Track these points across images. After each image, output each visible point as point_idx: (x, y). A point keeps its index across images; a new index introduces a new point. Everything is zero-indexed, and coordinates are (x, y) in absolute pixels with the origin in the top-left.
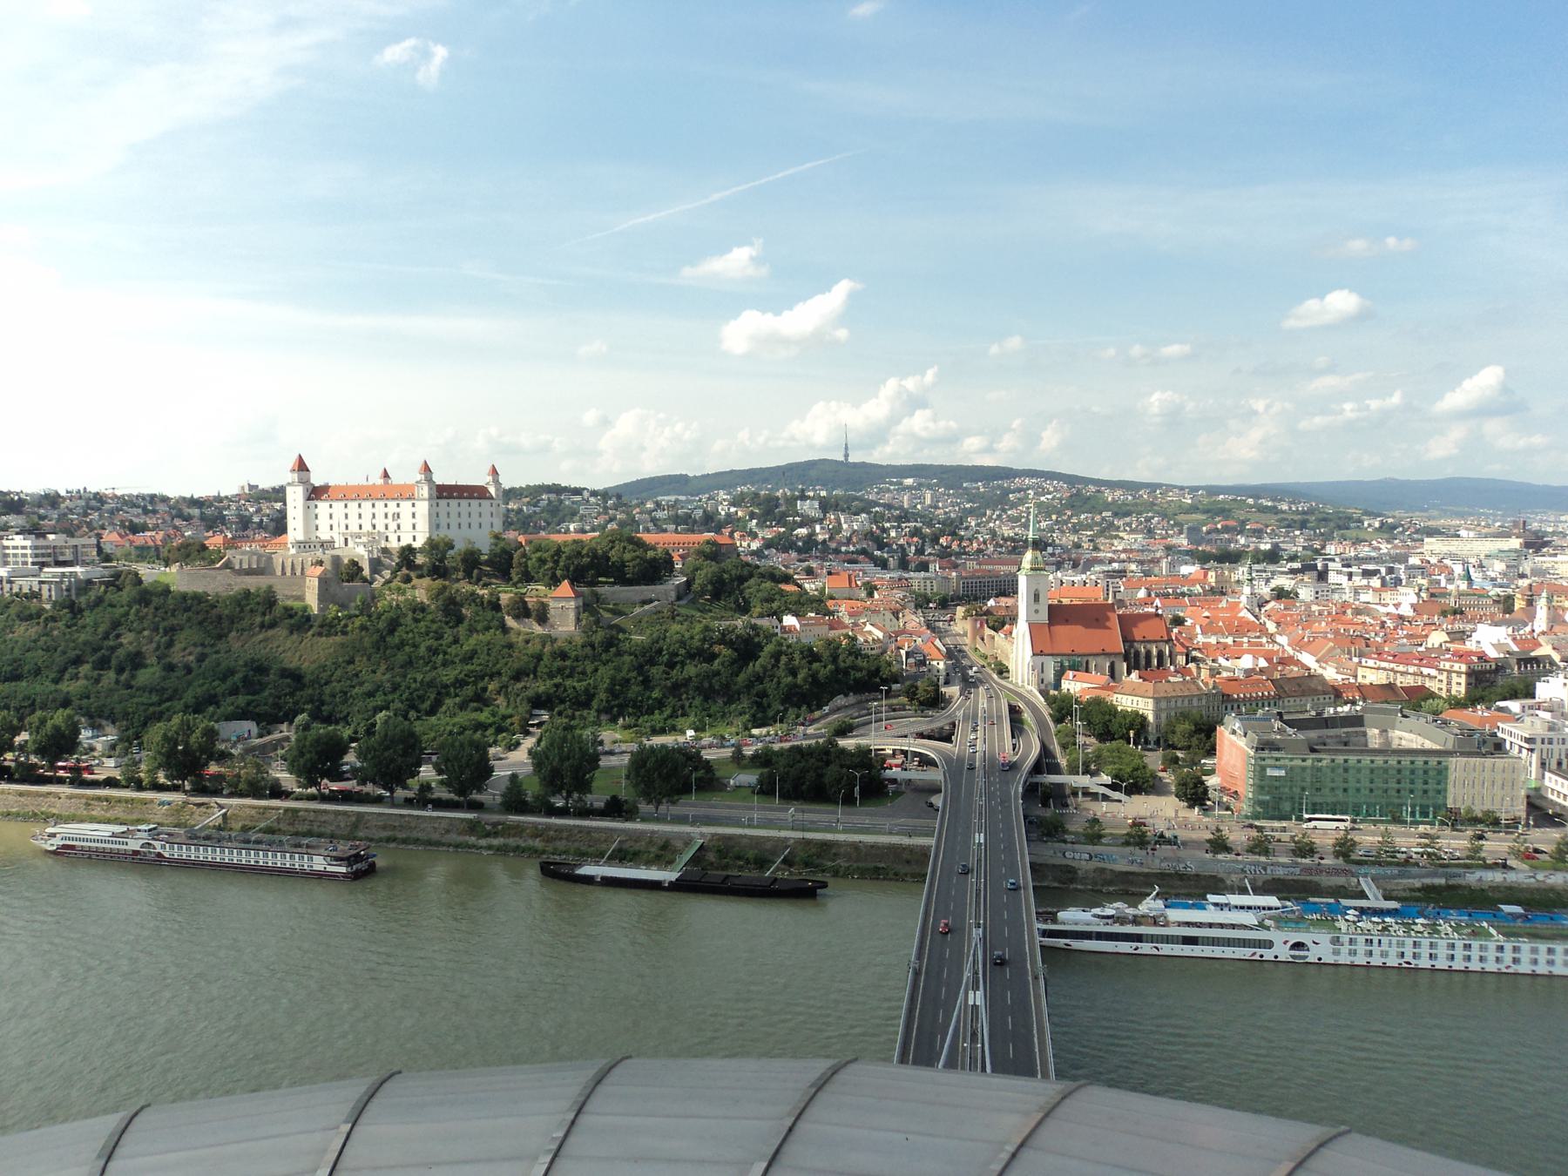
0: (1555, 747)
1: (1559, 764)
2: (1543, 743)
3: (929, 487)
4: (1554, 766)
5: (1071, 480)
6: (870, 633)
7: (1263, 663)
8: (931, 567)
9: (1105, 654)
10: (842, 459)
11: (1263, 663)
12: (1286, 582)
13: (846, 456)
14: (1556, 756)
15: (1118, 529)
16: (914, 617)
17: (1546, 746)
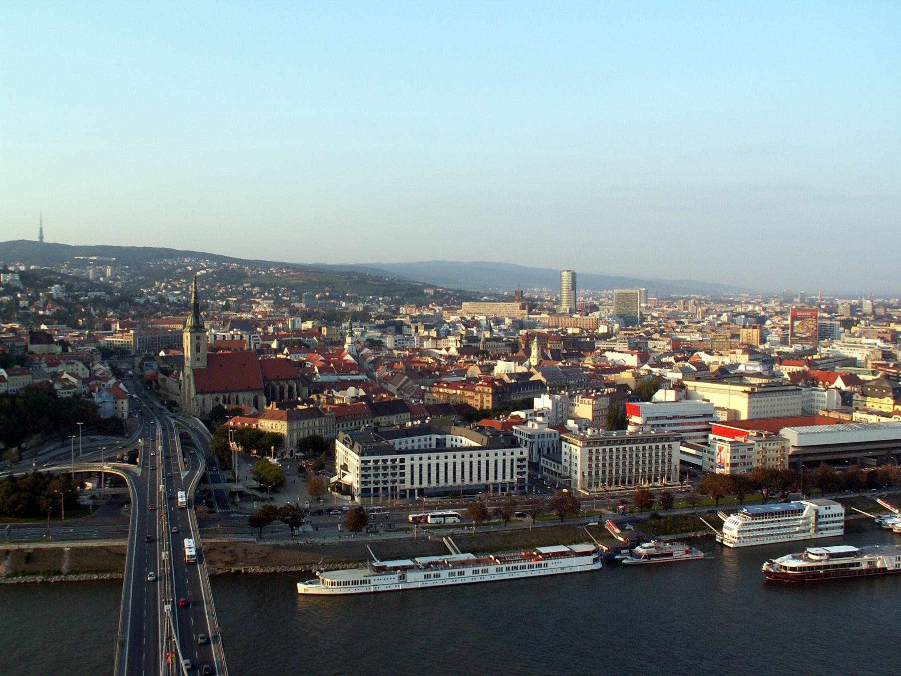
0: (546, 440)
1: (548, 450)
2: (539, 437)
3: (109, 263)
4: (545, 452)
5: (220, 259)
6: (67, 380)
7: (362, 393)
8: (113, 326)
9: (249, 390)
10: (38, 240)
11: (362, 393)
12: (375, 334)
13: (41, 237)
14: (546, 446)
15: (254, 296)
16: (102, 367)
17: (540, 440)
